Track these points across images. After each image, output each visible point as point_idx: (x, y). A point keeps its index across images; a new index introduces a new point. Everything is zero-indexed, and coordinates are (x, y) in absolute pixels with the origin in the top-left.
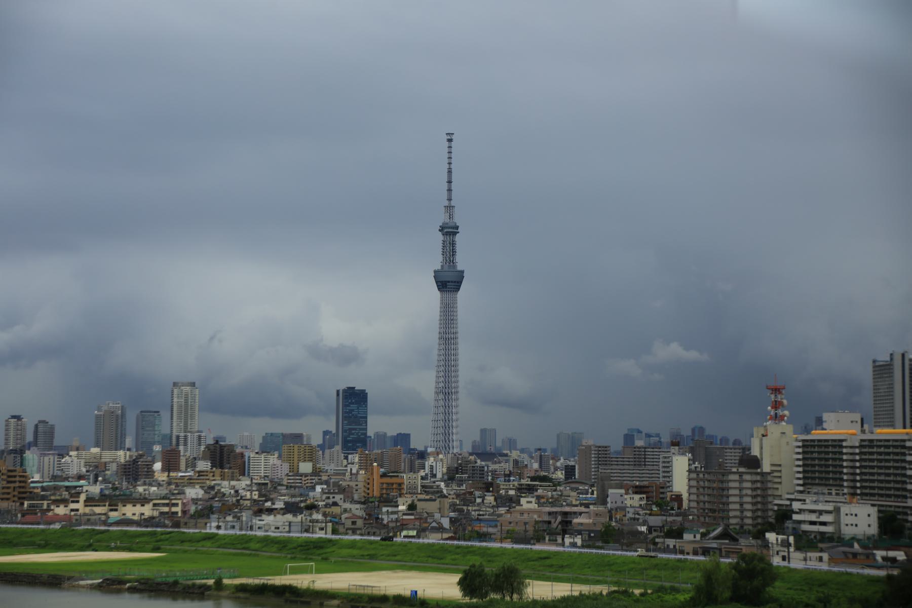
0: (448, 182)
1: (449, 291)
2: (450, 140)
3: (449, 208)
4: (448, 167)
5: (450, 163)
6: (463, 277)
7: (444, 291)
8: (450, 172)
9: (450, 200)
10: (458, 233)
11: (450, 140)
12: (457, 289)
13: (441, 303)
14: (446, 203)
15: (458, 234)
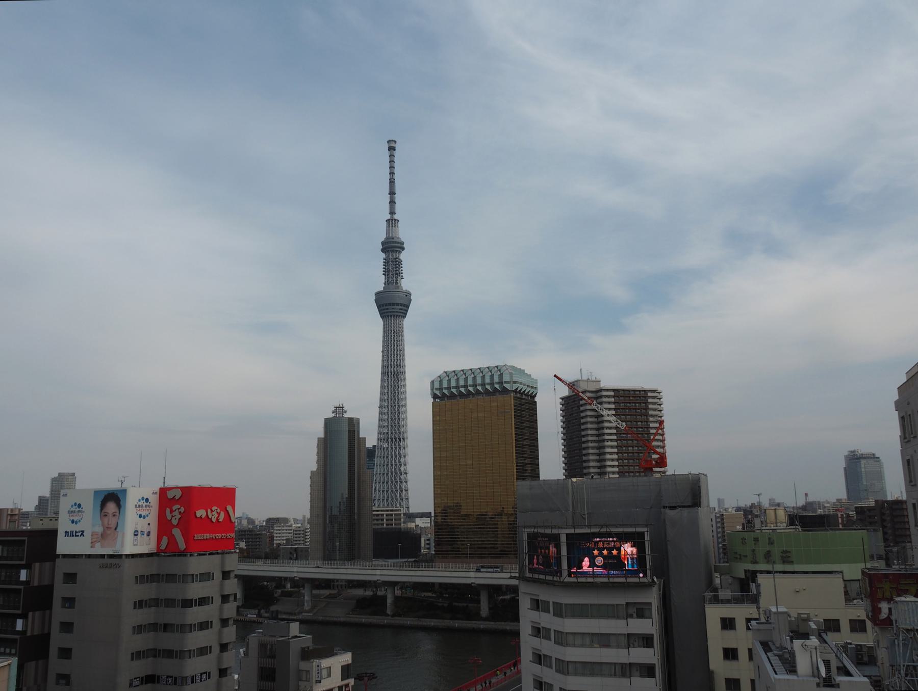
0: (389, 194)
1: (397, 316)
2: (392, 149)
3: (392, 223)
4: (389, 178)
5: (392, 173)
6: (411, 300)
7: (391, 316)
8: (392, 182)
9: (392, 212)
10: (403, 249)
11: (392, 149)
12: (404, 315)
13: (384, 332)
14: (389, 217)
15: (403, 252)
